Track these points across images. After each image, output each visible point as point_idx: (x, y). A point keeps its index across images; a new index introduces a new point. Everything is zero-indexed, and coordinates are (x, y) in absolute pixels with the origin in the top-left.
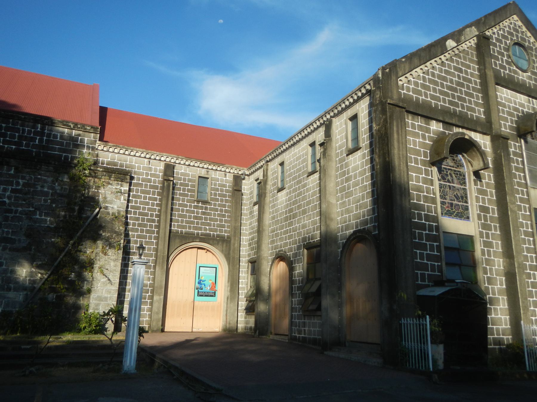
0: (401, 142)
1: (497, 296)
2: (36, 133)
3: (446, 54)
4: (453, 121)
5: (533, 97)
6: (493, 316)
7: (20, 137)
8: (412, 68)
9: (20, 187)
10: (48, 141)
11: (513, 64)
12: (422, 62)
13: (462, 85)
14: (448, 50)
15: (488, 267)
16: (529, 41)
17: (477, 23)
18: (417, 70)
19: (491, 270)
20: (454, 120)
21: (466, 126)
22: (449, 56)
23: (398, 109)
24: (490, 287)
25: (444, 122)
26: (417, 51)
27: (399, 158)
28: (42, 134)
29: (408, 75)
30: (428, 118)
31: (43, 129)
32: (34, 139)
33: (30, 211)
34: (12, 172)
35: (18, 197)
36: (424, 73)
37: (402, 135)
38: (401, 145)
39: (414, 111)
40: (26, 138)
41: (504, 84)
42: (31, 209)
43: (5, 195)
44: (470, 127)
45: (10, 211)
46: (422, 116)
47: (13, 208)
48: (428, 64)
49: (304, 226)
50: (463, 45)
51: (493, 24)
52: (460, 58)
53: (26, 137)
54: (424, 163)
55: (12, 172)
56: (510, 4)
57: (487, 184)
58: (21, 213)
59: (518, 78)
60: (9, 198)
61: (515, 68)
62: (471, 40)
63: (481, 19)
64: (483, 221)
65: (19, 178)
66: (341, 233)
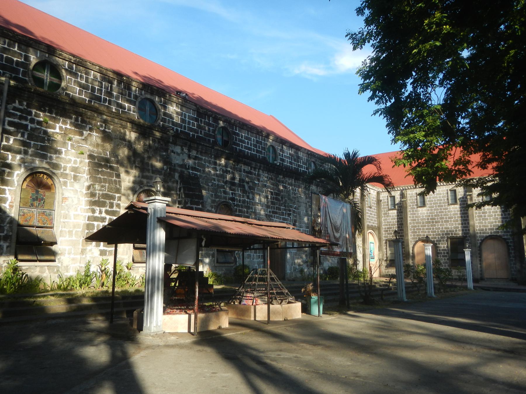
49: (445, 228)
66: (479, 235)
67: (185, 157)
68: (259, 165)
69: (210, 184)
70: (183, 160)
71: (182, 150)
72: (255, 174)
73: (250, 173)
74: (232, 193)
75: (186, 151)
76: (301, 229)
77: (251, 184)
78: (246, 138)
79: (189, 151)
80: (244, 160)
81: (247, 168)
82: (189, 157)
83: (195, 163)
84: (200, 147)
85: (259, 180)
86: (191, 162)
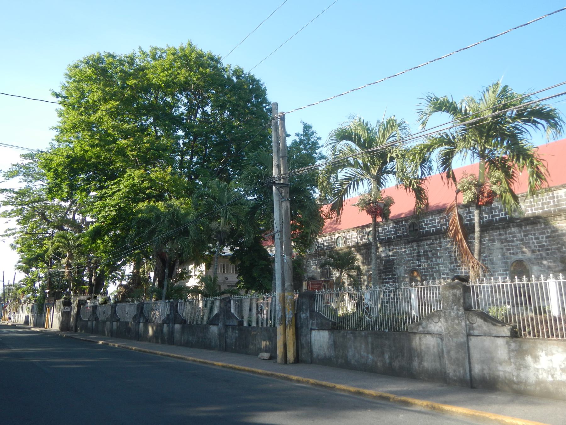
2: (550, 198)
7: (543, 204)
9: (549, 235)
10: (558, 201)
28: (553, 197)
31: (553, 194)
32: (549, 203)
33: (559, 247)
34: (543, 226)
35: (550, 240)
40: (545, 204)
42: (559, 246)
43: (543, 241)
45: (548, 249)
47: (549, 247)
53: (545, 202)
55: (543, 226)
58: (555, 249)
60: (546, 242)
65: (547, 229)
67: (387, 251)
68: (438, 236)
69: (403, 261)
70: (386, 253)
71: (386, 248)
72: (436, 244)
73: (432, 244)
74: (418, 262)
75: (387, 248)
76: (496, 273)
77: (434, 251)
78: (430, 220)
79: (389, 247)
80: (424, 238)
81: (429, 242)
82: (390, 251)
83: (393, 253)
84: (394, 243)
85: (440, 246)
86: (391, 253)
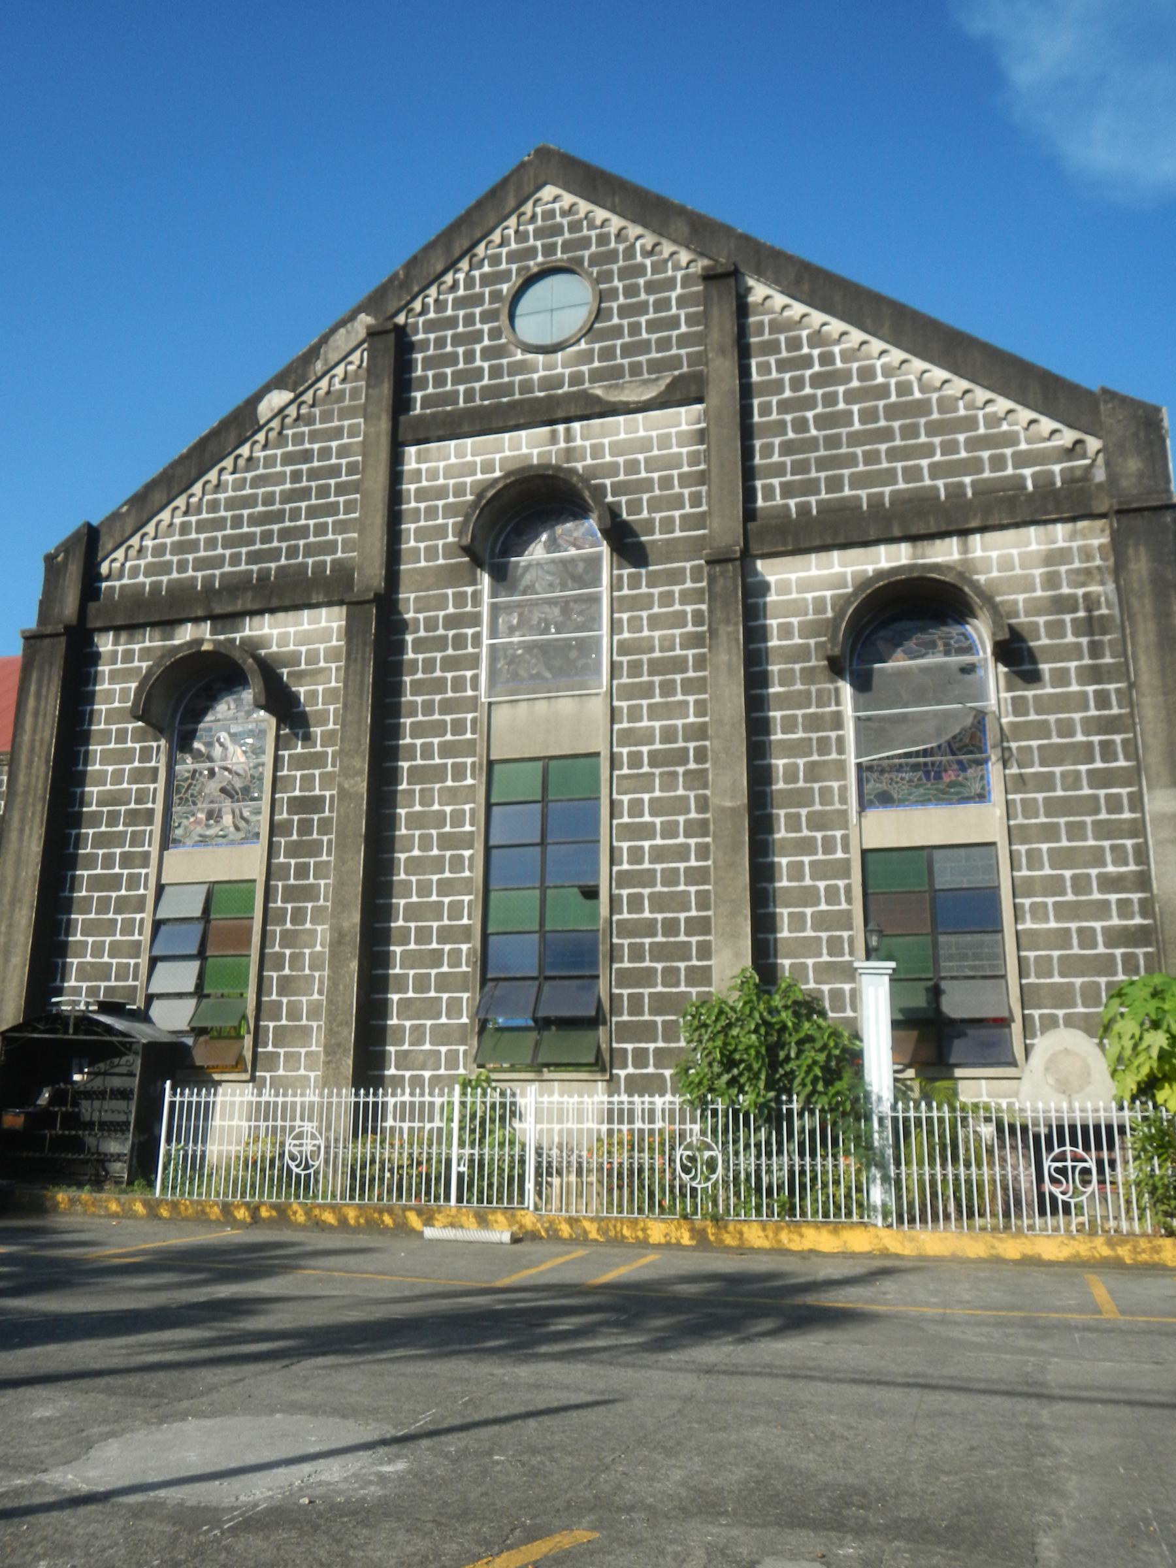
0: (41, 713)
1: (304, 1022)
3: (261, 437)
4: (239, 606)
5: (568, 420)
6: (281, 1072)
8: (145, 518)
11: (512, 348)
12: (175, 491)
13: (305, 494)
14: (262, 422)
15: (288, 952)
16: (603, 239)
17: (373, 303)
18: (165, 515)
19: (296, 959)
20: (240, 602)
21: (275, 603)
22: (273, 435)
23: (47, 641)
24: (285, 1000)
25: (213, 617)
26: (165, 472)
27: (32, 750)
29: (135, 541)
30: (168, 624)
36: (186, 513)
37: (47, 698)
38: (40, 720)
39: (127, 622)
41: (441, 433)
44: (287, 603)
46: (153, 625)
48: (197, 488)
50: (324, 384)
51: (439, 267)
52: (310, 420)
54: (139, 736)
56: (523, 165)
57: (329, 738)
59: (526, 387)
61: (519, 356)
62: (355, 357)
63: (395, 276)
64: (295, 837)
